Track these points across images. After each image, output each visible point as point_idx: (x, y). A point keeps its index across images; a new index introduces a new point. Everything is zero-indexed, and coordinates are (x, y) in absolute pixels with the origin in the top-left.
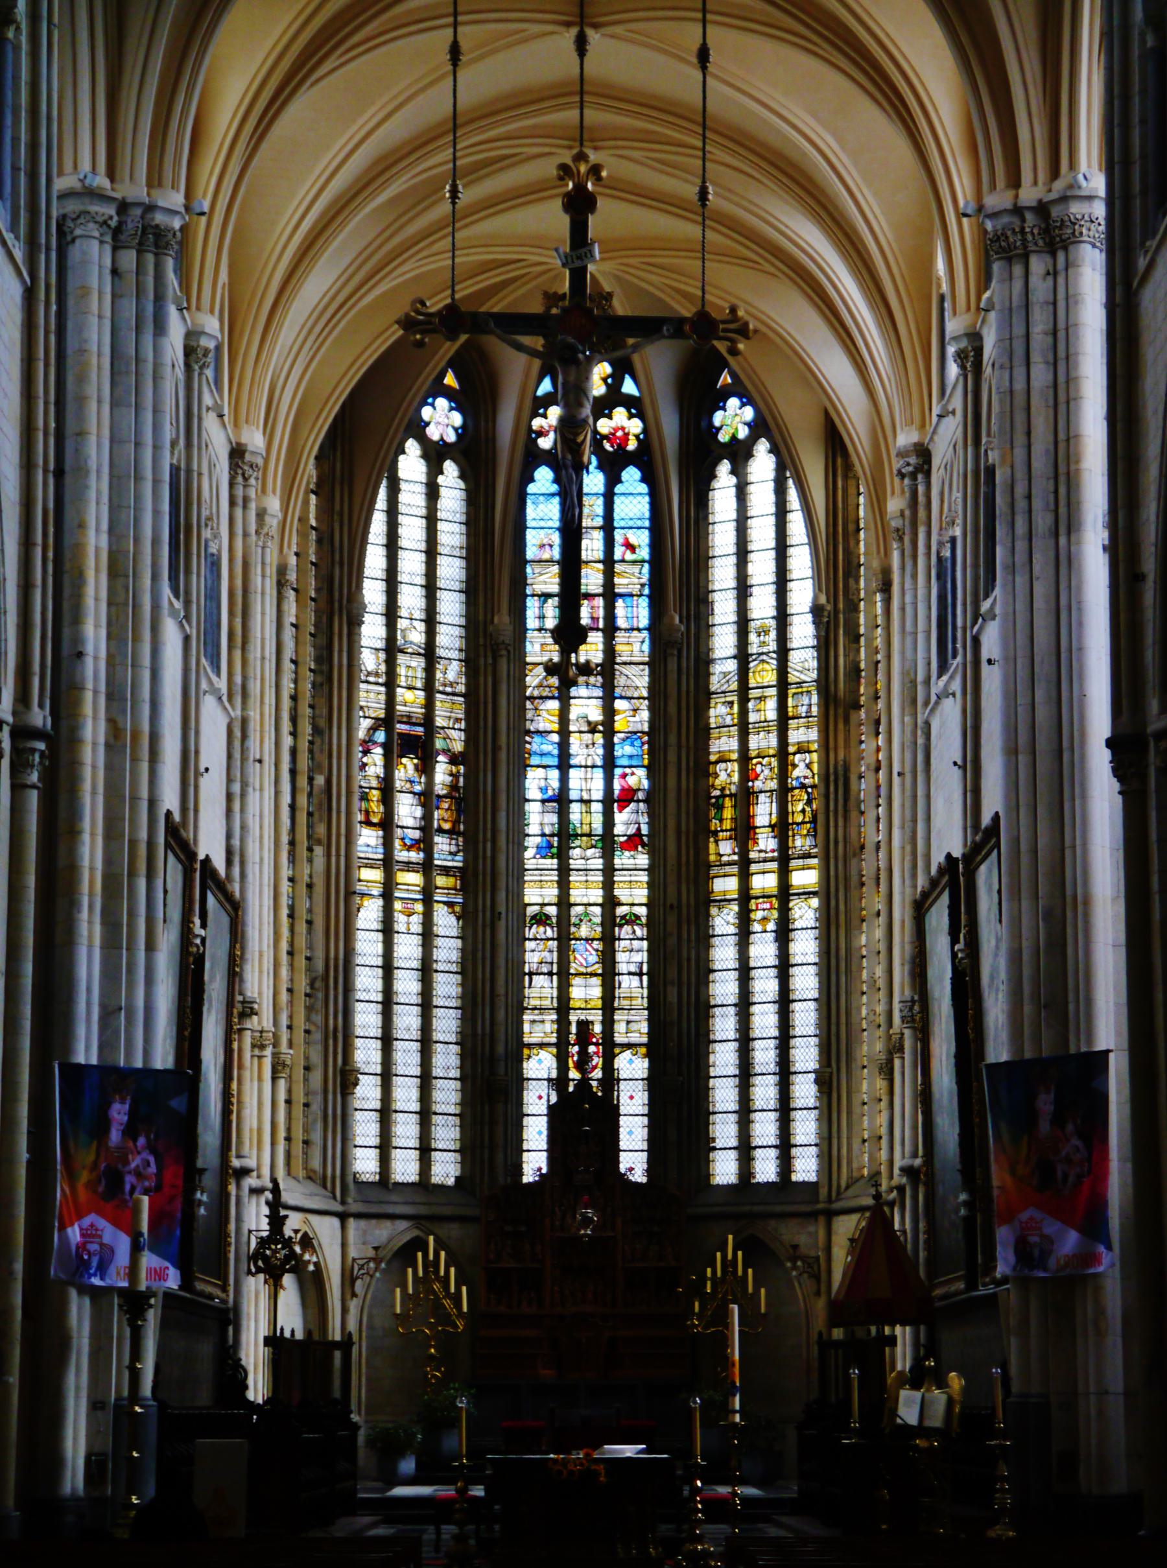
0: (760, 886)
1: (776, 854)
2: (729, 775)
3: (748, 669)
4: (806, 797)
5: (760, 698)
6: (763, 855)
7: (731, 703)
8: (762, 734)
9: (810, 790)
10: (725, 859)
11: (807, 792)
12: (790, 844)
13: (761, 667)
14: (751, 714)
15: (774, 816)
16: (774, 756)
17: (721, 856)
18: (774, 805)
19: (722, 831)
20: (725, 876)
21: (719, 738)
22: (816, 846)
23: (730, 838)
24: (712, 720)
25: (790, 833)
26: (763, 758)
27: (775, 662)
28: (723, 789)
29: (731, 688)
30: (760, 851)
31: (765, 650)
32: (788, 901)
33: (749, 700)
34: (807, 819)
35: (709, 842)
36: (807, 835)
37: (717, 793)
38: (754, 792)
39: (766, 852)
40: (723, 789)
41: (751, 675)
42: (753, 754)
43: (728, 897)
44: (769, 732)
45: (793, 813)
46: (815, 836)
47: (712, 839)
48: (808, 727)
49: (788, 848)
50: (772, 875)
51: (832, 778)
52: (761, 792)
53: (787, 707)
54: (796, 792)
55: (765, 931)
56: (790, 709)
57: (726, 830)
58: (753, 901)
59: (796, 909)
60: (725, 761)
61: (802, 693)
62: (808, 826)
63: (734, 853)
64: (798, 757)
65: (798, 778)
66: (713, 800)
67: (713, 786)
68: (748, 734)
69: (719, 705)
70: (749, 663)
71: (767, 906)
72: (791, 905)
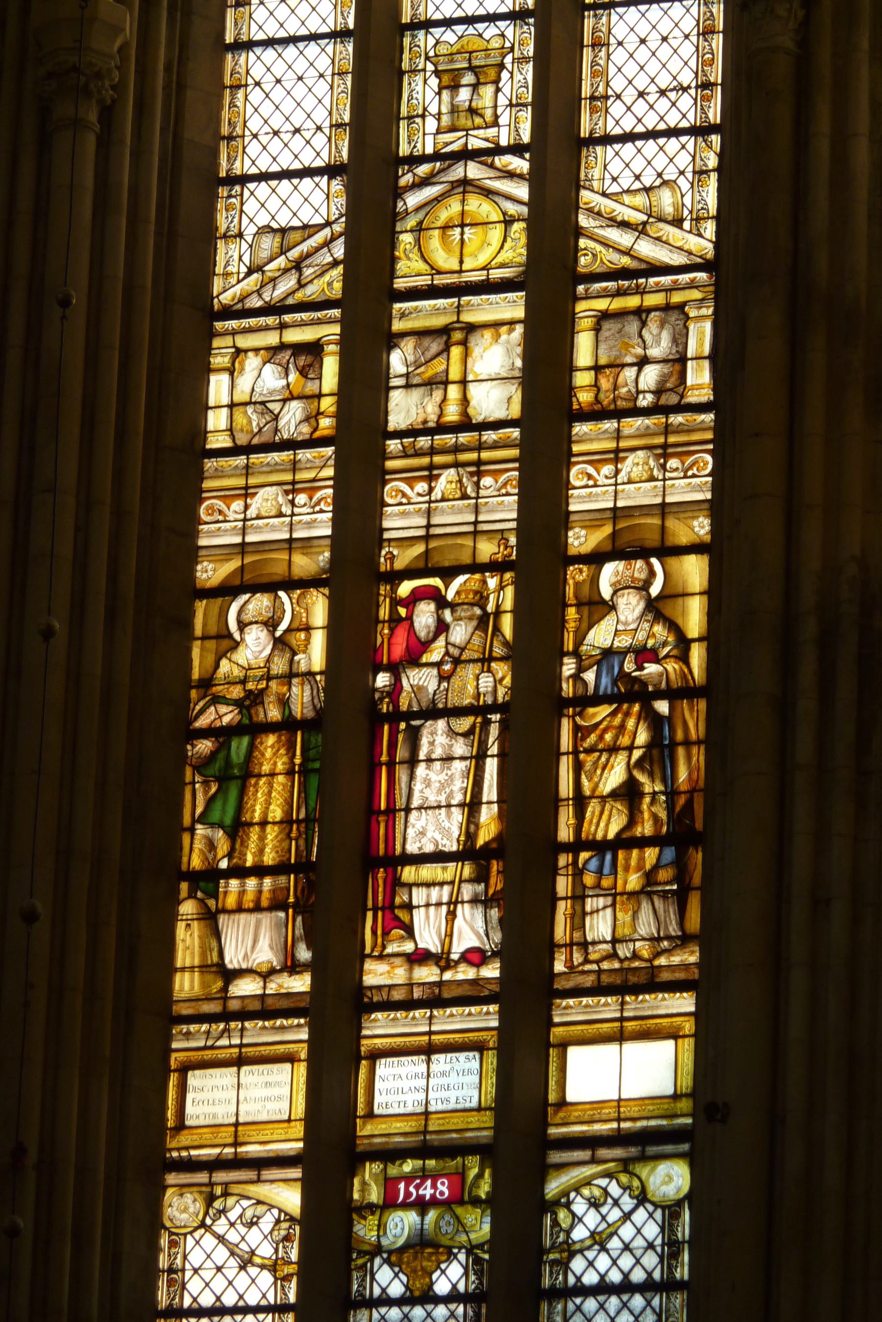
0: (412, 1102)
1: (492, 971)
2: (280, 643)
3: (395, 217)
4: (642, 737)
5: (445, 331)
6: (427, 974)
7: (315, 349)
8: (446, 481)
9: (662, 707)
10: (246, 987)
11: (655, 722)
12: (561, 932)
13: (452, 209)
14: (397, 398)
15: (488, 815)
16: (496, 567)
17: (230, 976)
18: (491, 766)
19: (239, 872)
20: (240, 1062)
21: (247, 492)
22: (684, 940)
23: (278, 904)
24: (217, 420)
25: (563, 885)
26: (448, 573)
27: (522, 191)
28: (254, 699)
29: (311, 292)
30: (420, 957)
31: (475, 143)
32: (543, 1171)
33: (392, 340)
34: (646, 828)
35: (172, 918)
36: (646, 891)
37: (228, 716)
38: (396, 716)
39: (443, 961)
40: (254, 699)
41: (406, 239)
42: (404, 558)
43: (252, 1150)
44: (479, 469)
45: (580, 801)
46: (681, 899)
47: (188, 908)
48: (664, 452)
49: (552, 947)
50: (468, 1061)
51: (809, 629)
52: (432, 713)
53: (571, 368)
54: (602, 712)
55: (428, 1298)
56: (582, 379)
57: (260, 871)
58: (372, 1169)
59: (580, 1206)
60: (271, 587)
61: (641, 313)
62: (651, 854)
63: (292, 967)
64: (610, 572)
65: (608, 653)
66: (204, 746)
67: (207, 683)
68: (382, 476)
69: (252, 362)
70: (398, 193)
71: (444, 1188)
72: (553, 1187)
